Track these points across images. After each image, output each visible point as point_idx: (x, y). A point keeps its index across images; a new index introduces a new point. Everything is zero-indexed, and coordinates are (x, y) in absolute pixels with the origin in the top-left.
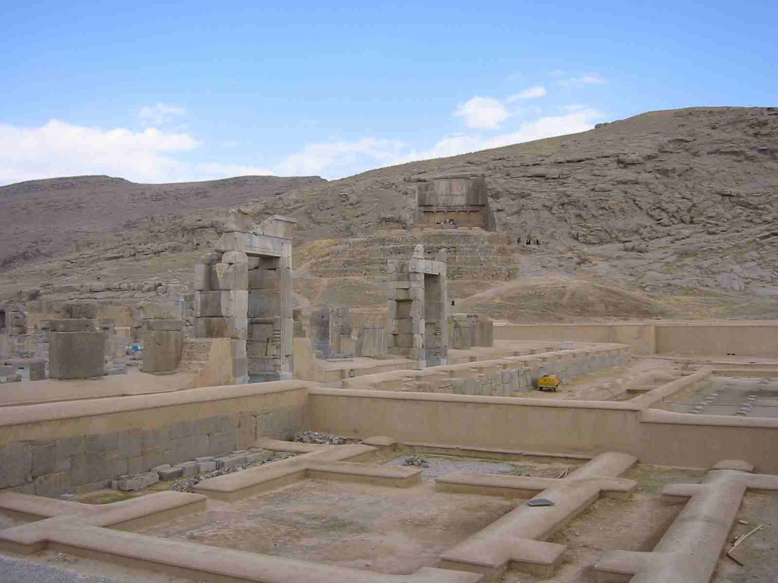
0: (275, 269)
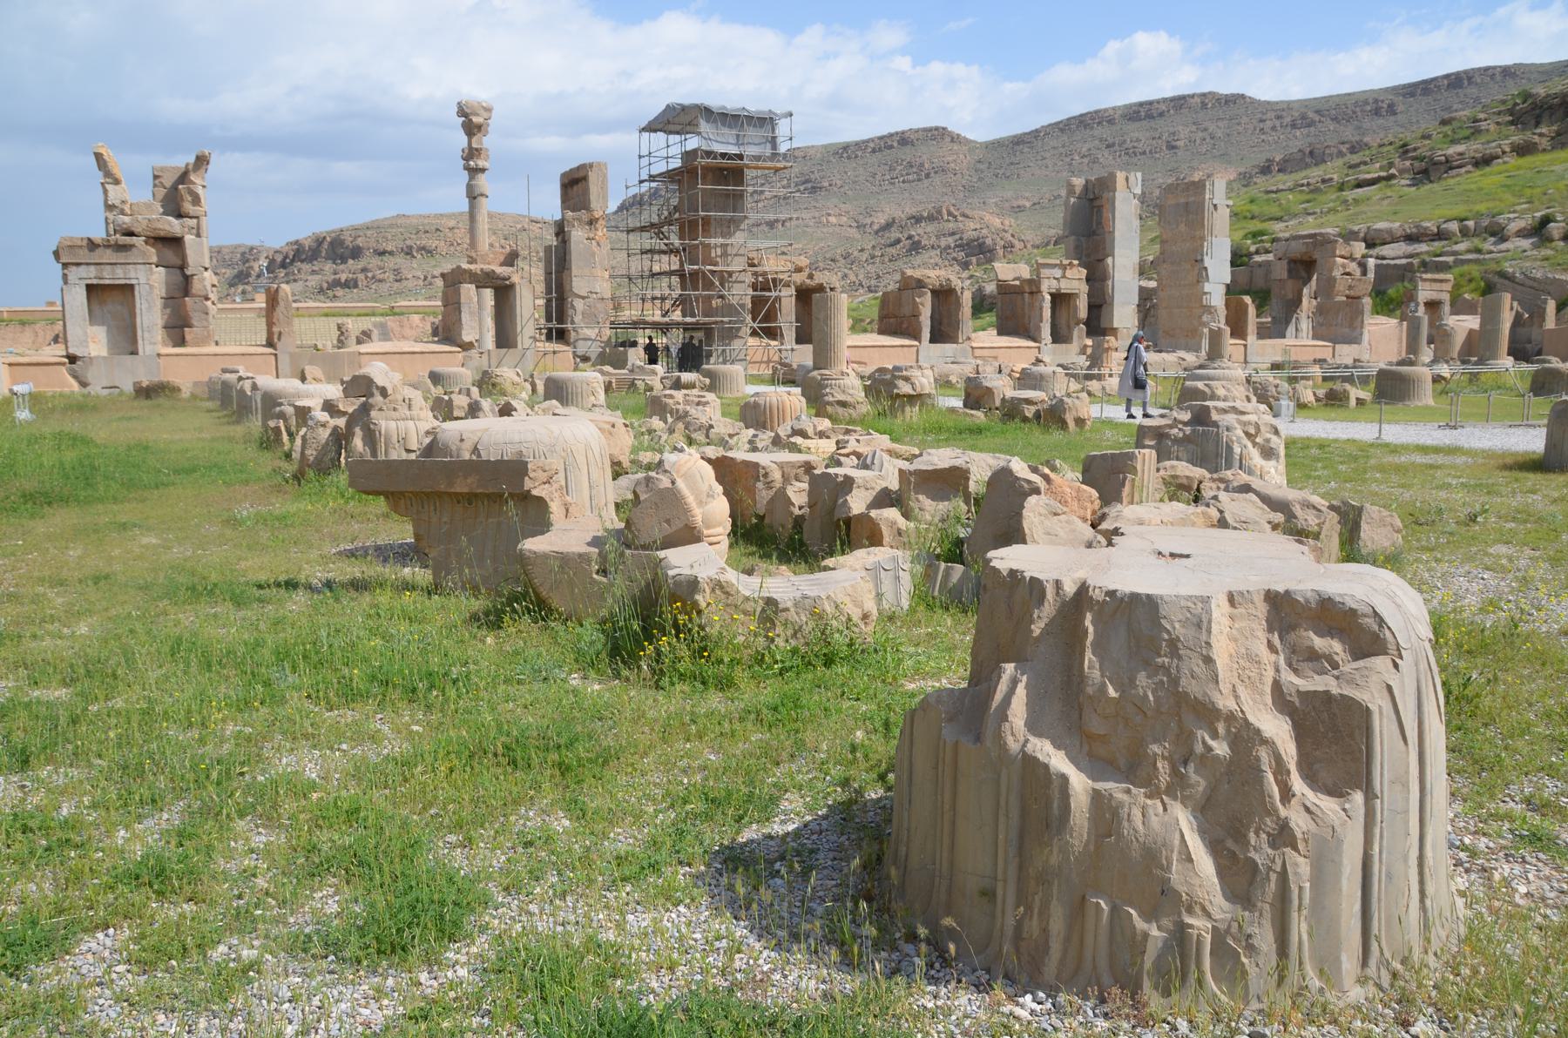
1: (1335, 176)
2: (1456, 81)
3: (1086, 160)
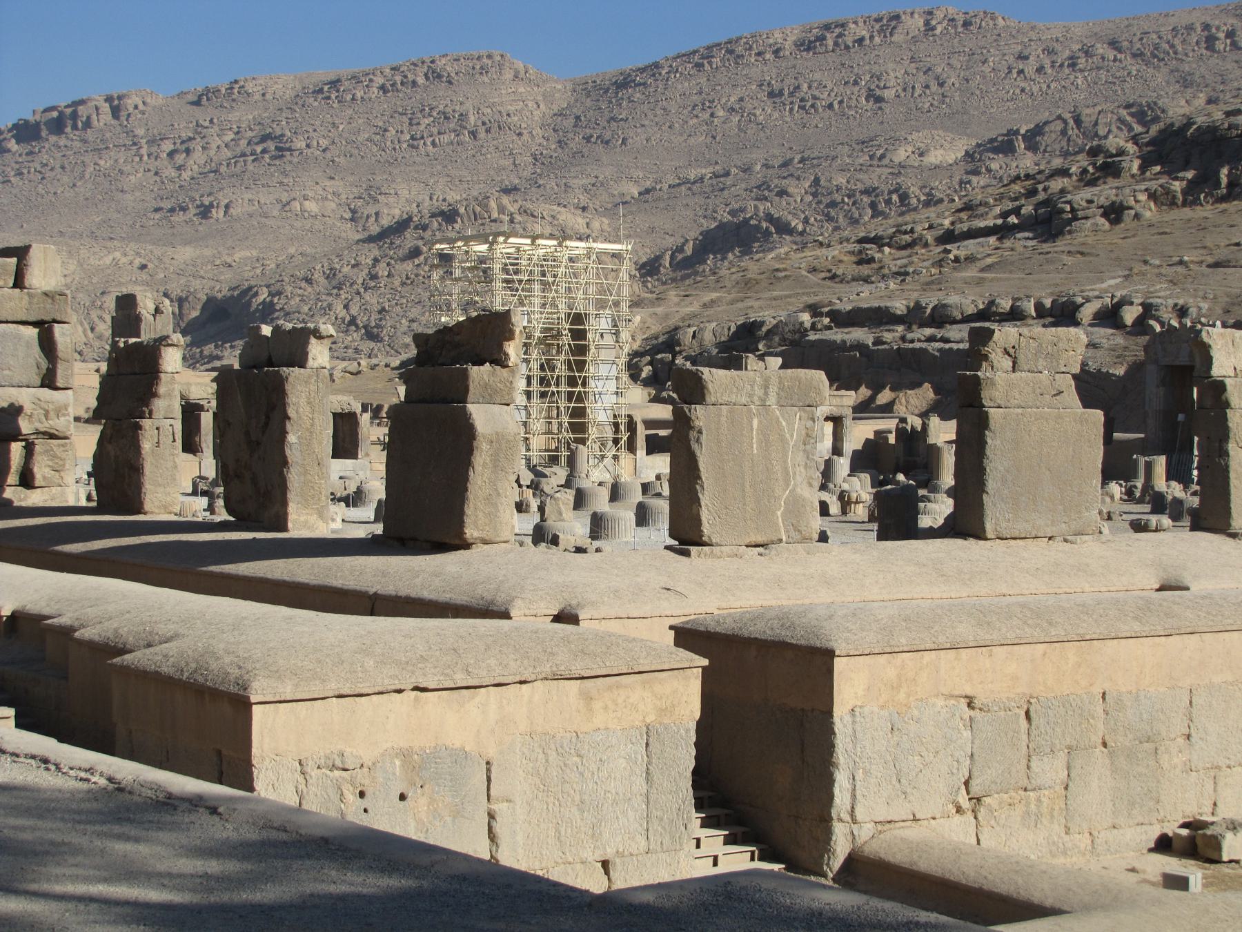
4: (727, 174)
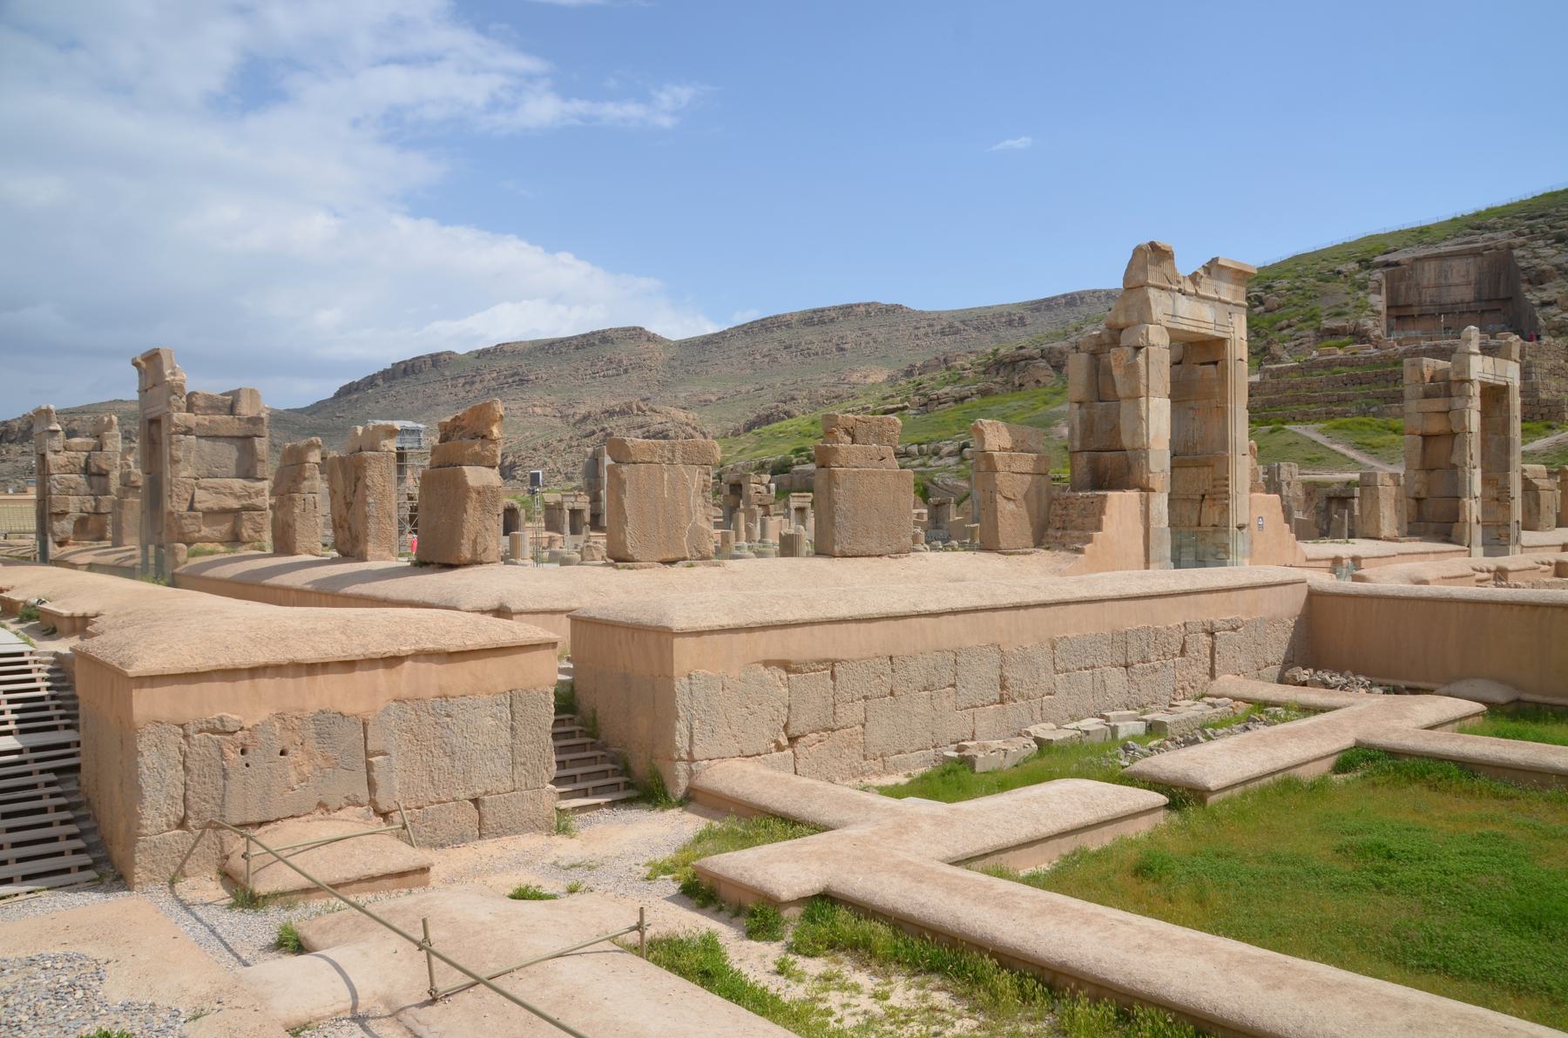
0: (1216, 363)
1: (871, 406)
2: (1072, 300)
3: (767, 360)
4: (762, 389)
